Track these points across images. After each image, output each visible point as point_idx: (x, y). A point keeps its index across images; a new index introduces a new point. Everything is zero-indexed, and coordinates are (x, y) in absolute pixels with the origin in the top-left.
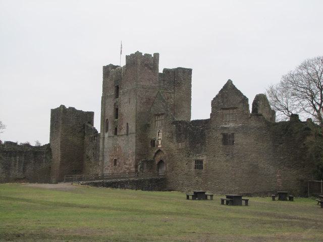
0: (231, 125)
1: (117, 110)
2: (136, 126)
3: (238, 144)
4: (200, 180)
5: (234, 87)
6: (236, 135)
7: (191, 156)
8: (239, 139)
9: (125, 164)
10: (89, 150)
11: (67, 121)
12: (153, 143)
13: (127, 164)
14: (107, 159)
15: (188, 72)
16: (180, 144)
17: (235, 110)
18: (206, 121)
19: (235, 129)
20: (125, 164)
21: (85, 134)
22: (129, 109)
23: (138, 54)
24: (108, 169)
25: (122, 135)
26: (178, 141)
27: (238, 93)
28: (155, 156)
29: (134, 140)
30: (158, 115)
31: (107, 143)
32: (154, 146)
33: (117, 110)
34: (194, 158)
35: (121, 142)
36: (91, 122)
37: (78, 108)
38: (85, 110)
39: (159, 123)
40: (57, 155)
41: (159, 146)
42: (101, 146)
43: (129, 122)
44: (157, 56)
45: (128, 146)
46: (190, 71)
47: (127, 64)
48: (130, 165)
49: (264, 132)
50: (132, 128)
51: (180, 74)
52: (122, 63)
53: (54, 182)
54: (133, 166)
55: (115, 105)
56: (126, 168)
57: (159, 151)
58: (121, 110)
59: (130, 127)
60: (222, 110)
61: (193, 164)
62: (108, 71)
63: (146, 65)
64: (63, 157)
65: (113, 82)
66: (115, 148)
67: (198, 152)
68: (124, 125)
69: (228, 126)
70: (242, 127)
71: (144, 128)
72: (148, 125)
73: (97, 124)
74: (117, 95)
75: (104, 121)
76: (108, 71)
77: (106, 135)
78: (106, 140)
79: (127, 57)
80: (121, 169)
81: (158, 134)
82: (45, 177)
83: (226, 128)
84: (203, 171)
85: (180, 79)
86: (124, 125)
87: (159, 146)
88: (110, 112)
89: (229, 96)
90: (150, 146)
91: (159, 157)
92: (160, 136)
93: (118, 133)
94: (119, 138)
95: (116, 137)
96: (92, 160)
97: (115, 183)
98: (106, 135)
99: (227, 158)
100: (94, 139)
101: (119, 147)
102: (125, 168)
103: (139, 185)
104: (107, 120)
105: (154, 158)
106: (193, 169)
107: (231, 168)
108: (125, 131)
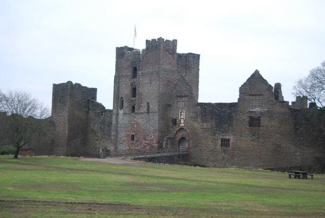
0: (258, 109)
1: (134, 90)
2: (159, 105)
3: (263, 126)
4: (226, 156)
5: (261, 77)
6: (262, 119)
7: (217, 135)
8: (264, 121)
10: (95, 124)
11: (72, 96)
12: (175, 122)
14: (122, 135)
15: (196, 57)
16: (205, 124)
17: (261, 97)
18: (232, 105)
19: (261, 113)
21: (89, 108)
22: (150, 90)
23: (160, 39)
24: (123, 144)
25: (142, 113)
26: (203, 121)
27: (265, 82)
28: (176, 133)
29: (156, 118)
30: (181, 97)
31: (123, 118)
32: (176, 124)
33: (134, 90)
34: (221, 137)
35: (140, 120)
36: (95, 97)
37: (83, 85)
38: (90, 85)
39: (181, 104)
40: (63, 129)
41: (181, 125)
42: (114, 122)
44: (175, 42)
45: (150, 124)
46: (199, 56)
47: (147, 48)
49: (287, 116)
50: (154, 107)
51: (191, 59)
52: (141, 46)
53: (102, 157)
54: (155, 141)
55: (132, 84)
56: (148, 144)
57: (182, 129)
58: (140, 90)
59: (151, 106)
60: (249, 97)
61: (219, 142)
62: (122, 53)
63: (167, 50)
64: (70, 130)
65: (129, 63)
66: (132, 125)
67: (226, 132)
69: (256, 110)
70: (268, 112)
71: (166, 107)
72: (170, 106)
73: (106, 99)
74: (135, 75)
75: (118, 98)
76: (122, 53)
77: (121, 112)
78: (120, 117)
79: (147, 41)
81: (181, 114)
82: (49, 149)
83: (253, 112)
84: (230, 149)
85: (191, 62)
86: (144, 104)
87: (181, 125)
88: (126, 91)
89: (255, 85)
90: (171, 124)
91: (180, 135)
92: (183, 117)
93: (136, 111)
96: (99, 134)
97: (154, 158)
98: (121, 112)
99: (253, 138)
100: (102, 115)
101: (138, 124)
103: (171, 160)
104: (122, 97)
105: (175, 136)
106: (219, 147)
107: (256, 147)
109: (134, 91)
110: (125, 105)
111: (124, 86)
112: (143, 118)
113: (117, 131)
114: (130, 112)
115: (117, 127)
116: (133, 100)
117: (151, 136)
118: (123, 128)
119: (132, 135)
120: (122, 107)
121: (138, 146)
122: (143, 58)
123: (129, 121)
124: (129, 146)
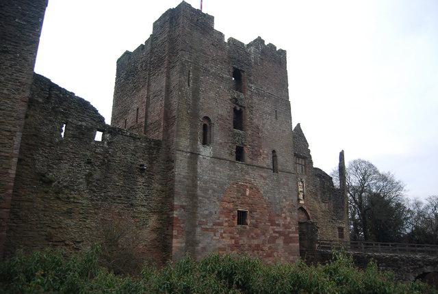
9: (273, 223)
13: (278, 225)
20: (273, 223)
24: (215, 231)
43: (275, 148)
48: (286, 226)
54: (293, 228)
59: (280, 159)
68: (266, 151)
77: (206, 152)
80: (264, 234)
86: (266, 151)
93: (248, 160)
94: (250, 171)
95: (239, 165)
102: (275, 232)
108: (269, 162)
109: (238, 118)
110: (218, 136)
111: (212, 94)
112: (265, 179)
113: (193, 196)
114: (233, 158)
115: (195, 186)
116: (239, 135)
117: (285, 218)
118: (214, 191)
119: (238, 211)
120: (205, 143)
121: (258, 236)
122: (256, 63)
123: (230, 177)
124: (232, 238)
